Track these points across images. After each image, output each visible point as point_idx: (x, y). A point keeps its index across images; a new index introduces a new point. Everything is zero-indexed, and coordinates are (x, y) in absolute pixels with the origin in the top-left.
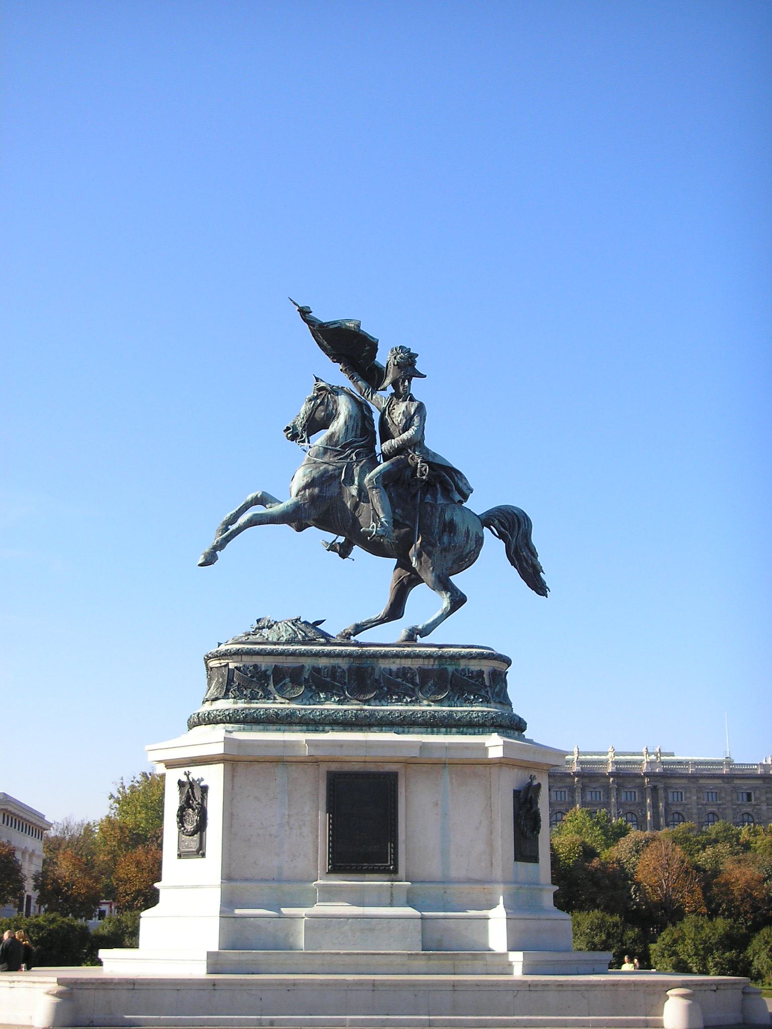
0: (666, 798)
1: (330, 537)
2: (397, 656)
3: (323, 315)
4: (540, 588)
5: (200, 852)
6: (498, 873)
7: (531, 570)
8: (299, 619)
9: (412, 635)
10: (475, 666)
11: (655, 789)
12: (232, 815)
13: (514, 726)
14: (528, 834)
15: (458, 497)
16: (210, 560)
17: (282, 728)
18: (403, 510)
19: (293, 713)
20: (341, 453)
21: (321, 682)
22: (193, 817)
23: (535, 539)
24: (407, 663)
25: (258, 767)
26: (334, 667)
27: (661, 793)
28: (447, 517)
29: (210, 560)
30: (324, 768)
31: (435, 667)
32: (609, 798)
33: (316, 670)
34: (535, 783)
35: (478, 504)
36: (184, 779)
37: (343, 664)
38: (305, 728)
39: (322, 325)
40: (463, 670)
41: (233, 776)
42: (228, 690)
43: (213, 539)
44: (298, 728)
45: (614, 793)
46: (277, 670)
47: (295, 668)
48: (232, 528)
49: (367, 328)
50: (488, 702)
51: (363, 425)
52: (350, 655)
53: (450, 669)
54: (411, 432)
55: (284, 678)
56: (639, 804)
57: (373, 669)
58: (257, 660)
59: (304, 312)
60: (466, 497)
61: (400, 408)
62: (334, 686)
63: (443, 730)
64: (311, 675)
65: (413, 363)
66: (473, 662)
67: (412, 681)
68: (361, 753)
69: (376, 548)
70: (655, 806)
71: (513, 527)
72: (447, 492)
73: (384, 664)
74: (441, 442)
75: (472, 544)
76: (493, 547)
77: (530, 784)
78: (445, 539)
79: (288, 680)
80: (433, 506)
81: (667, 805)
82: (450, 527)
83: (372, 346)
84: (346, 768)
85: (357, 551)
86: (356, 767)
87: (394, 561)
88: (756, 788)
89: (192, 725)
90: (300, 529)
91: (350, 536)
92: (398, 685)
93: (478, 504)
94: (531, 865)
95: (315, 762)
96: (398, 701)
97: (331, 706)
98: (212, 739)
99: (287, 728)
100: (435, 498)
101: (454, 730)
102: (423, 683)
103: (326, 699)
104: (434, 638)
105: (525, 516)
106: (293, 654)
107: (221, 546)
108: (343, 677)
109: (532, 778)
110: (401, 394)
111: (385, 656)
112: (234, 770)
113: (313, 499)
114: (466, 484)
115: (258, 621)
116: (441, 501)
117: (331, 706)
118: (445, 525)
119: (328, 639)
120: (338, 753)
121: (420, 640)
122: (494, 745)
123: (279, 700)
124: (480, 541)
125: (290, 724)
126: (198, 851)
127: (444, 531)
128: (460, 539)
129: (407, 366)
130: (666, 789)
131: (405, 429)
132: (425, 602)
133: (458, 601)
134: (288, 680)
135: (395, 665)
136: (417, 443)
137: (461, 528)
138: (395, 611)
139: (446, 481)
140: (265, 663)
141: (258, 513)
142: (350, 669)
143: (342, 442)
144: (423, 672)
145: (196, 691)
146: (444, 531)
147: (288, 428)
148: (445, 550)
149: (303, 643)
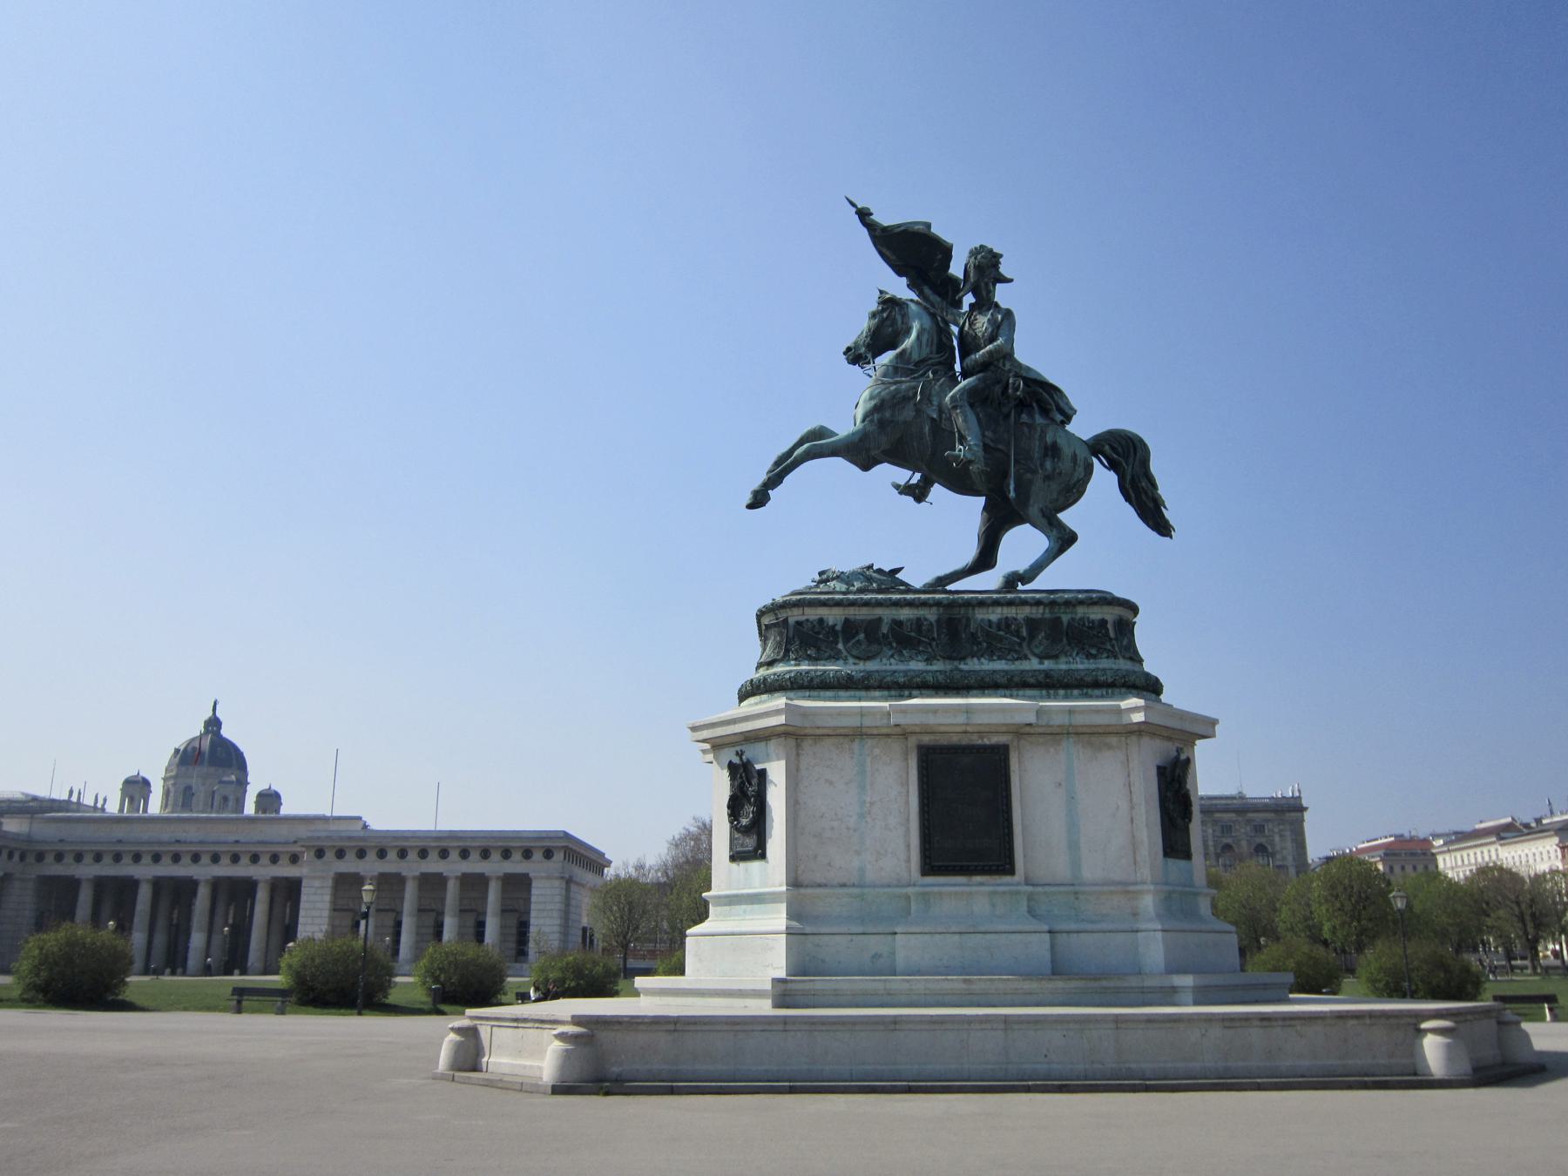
1: (903, 475)
2: (996, 603)
3: (886, 217)
4: (1161, 526)
5: (759, 853)
6: (1145, 872)
7: (1151, 505)
8: (871, 567)
9: (1012, 581)
10: (1096, 614)
12: (797, 802)
13: (1151, 687)
14: (1179, 821)
15: (1059, 418)
16: (759, 499)
17: (858, 693)
18: (994, 432)
19: (869, 674)
20: (913, 372)
21: (904, 639)
22: (750, 809)
23: (1154, 468)
24: (1010, 612)
25: (828, 741)
26: (918, 619)
28: (1049, 439)
29: (759, 499)
30: (913, 741)
31: (1047, 615)
33: (897, 624)
34: (1183, 757)
35: (1083, 427)
36: (736, 760)
37: (931, 615)
38: (886, 693)
39: (885, 229)
40: (1082, 619)
41: (798, 755)
42: (787, 651)
43: (762, 477)
44: (877, 693)
46: (847, 622)
47: (871, 622)
50: (1116, 657)
51: (940, 340)
52: (938, 604)
53: (1065, 618)
54: (1000, 341)
55: (857, 633)
57: (968, 620)
58: (822, 612)
60: (1068, 418)
61: (982, 323)
62: (920, 642)
63: (1061, 692)
64: (891, 629)
65: (996, 265)
66: (1096, 609)
67: (1017, 633)
68: (961, 719)
69: (961, 484)
71: (1125, 454)
72: (1045, 412)
73: (981, 615)
74: (1034, 350)
75: (1080, 471)
77: (1177, 758)
78: (1048, 465)
79: (862, 636)
80: (1031, 427)
82: (1053, 451)
83: (946, 252)
84: (943, 741)
85: (938, 491)
86: (955, 739)
87: (983, 499)
88: (1268, 821)
89: (743, 696)
90: (866, 467)
92: (1001, 639)
93: (1083, 427)
94: (1182, 863)
95: (903, 733)
96: (1000, 658)
97: (917, 665)
98: (771, 709)
99: (863, 693)
100: (1031, 416)
101: (1076, 692)
102: (1032, 636)
103: (911, 658)
104: (1043, 582)
105: (1141, 441)
106: (867, 604)
108: (930, 630)
109: (1179, 751)
110: (985, 302)
111: (982, 603)
112: (798, 746)
113: (882, 424)
114: (1068, 403)
115: (821, 574)
116: (1039, 420)
117: (917, 665)
118: (1046, 448)
119: (909, 589)
120: (931, 720)
121: (1020, 587)
122: (1133, 707)
123: (851, 660)
124: (1089, 470)
125: (868, 688)
126: (756, 850)
127: (1045, 455)
128: (1065, 465)
129: (987, 268)
131: (992, 339)
133: (1064, 540)
134: (862, 636)
135: (995, 615)
136: (1007, 355)
137: (1067, 451)
138: (986, 559)
139: (1044, 399)
140: (834, 616)
141: (816, 445)
142: (938, 621)
143: (915, 357)
144: (1032, 623)
145: (746, 654)
146: (1045, 455)
147: (849, 349)
148: (1048, 478)
149: (879, 591)
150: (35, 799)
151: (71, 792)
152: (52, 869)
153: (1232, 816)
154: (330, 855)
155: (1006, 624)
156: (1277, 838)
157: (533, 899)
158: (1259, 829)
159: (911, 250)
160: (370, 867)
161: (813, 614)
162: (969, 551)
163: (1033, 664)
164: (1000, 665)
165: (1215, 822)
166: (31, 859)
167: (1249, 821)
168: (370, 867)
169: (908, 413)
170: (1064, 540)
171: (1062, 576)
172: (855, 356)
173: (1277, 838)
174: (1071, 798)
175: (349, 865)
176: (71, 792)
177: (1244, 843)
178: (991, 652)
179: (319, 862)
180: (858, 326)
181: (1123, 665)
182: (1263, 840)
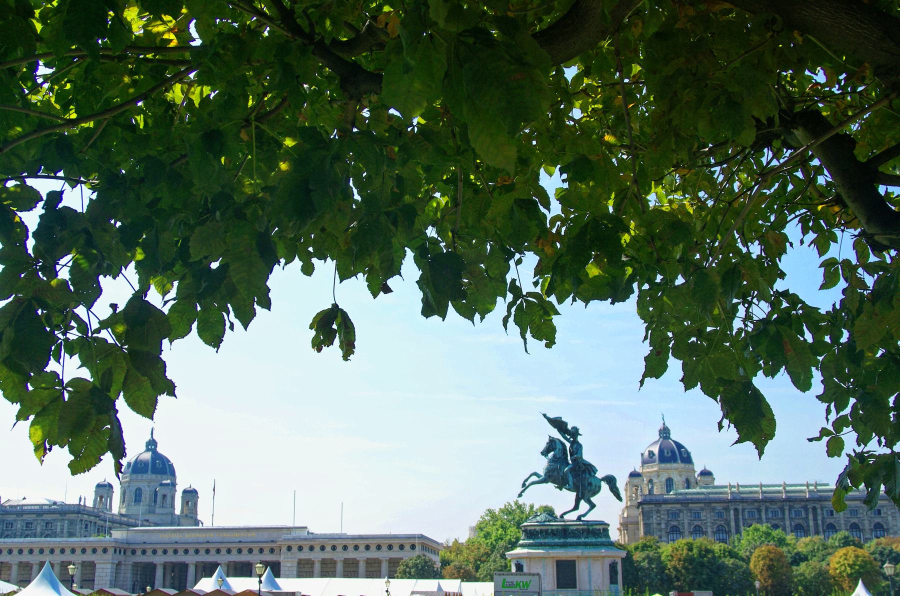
0: (823, 514)
3: (552, 416)
10: (598, 527)
11: (814, 509)
27: (819, 511)
45: (787, 512)
48: (527, 483)
56: (803, 519)
59: (545, 415)
70: (815, 519)
74: (588, 456)
76: (605, 486)
81: (823, 518)
91: (561, 484)
93: (599, 475)
97: (557, 540)
107: (523, 491)
117: (557, 540)
128: (593, 488)
130: (822, 508)
132: (584, 506)
135: (575, 528)
138: (576, 507)
139: (590, 469)
140: (538, 528)
144: (583, 530)
150: (63, 505)
151: (80, 499)
152: (140, 558)
155: (577, 530)
156: (890, 518)
159: (558, 424)
161: (533, 528)
163: (583, 540)
164: (575, 540)
166: (129, 553)
169: (556, 473)
170: (593, 506)
171: (592, 517)
172: (542, 453)
173: (890, 518)
174: (590, 572)
175: (305, 555)
176: (80, 499)
177: (866, 522)
178: (573, 537)
180: (543, 445)
181: (604, 540)
182: (879, 520)
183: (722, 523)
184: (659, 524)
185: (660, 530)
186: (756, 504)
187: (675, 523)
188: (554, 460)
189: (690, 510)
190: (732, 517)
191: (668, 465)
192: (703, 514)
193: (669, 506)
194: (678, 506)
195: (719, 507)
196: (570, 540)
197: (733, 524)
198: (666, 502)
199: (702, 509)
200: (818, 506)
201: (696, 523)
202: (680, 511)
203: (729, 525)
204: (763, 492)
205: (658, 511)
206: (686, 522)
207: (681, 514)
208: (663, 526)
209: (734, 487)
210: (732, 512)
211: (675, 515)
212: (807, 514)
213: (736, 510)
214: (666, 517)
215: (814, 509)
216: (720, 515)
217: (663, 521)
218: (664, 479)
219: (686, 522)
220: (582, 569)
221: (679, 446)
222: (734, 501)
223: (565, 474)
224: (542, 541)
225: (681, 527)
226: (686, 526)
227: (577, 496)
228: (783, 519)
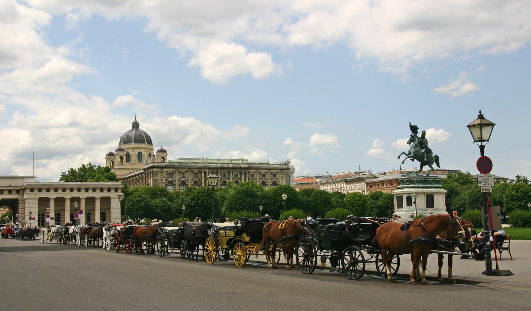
3: (412, 125)
11: (245, 173)
32: (229, 176)
35: (433, 155)
46: (417, 180)
49: (418, 127)
59: (410, 124)
71: (437, 158)
88: (277, 173)
93: (433, 155)
95: (424, 193)
140: (415, 179)
153: (266, 171)
154: (36, 191)
156: (280, 179)
157: (112, 205)
158: (275, 176)
160: (52, 195)
162: (419, 169)
165: (260, 173)
167: (271, 173)
168: (52, 195)
172: (408, 143)
175: (44, 194)
177: (269, 181)
178: (429, 184)
179: (32, 194)
182: (275, 180)
183: (196, 180)
184: (162, 180)
185: (162, 183)
186: (215, 170)
187: (171, 179)
188: (416, 146)
189: (180, 172)
190: (203, 176)
191: (139, 145)
192: (186, 174)
193: (167, 170)
194: (173, 170)
195: (196, 171)
196: (428, 185)
197: (203, 180)
198: (166, 167)
199: (186, 172)
200: (247, 172)
201: (182, 179)
202: (174, 172)
203: (200, 180)
204: (220, 163)
205: (162, 172)
206: (177, 178)
207: (174, 174)
208: (164, 181)
209: (205, 159)
210: (203, 174)
211: (171, 175)
212: (241, 176)
213: (205, 173)
214: (166, 176)
215: (245, 173)
216: (196, 175)
217: (164, 178)
218: (137, 154)
219: (177, 178)
220: (436, 198)
221: (146, 134)
222: (204, 168)
223: (423, 153)
224: (417, 185)
225: (174, 182)
226: (177, 181)
227: (421, 164)
228: (229, 178)
